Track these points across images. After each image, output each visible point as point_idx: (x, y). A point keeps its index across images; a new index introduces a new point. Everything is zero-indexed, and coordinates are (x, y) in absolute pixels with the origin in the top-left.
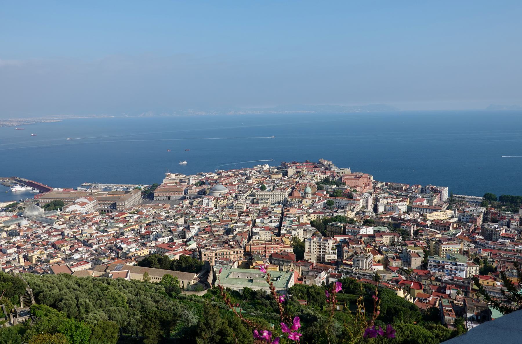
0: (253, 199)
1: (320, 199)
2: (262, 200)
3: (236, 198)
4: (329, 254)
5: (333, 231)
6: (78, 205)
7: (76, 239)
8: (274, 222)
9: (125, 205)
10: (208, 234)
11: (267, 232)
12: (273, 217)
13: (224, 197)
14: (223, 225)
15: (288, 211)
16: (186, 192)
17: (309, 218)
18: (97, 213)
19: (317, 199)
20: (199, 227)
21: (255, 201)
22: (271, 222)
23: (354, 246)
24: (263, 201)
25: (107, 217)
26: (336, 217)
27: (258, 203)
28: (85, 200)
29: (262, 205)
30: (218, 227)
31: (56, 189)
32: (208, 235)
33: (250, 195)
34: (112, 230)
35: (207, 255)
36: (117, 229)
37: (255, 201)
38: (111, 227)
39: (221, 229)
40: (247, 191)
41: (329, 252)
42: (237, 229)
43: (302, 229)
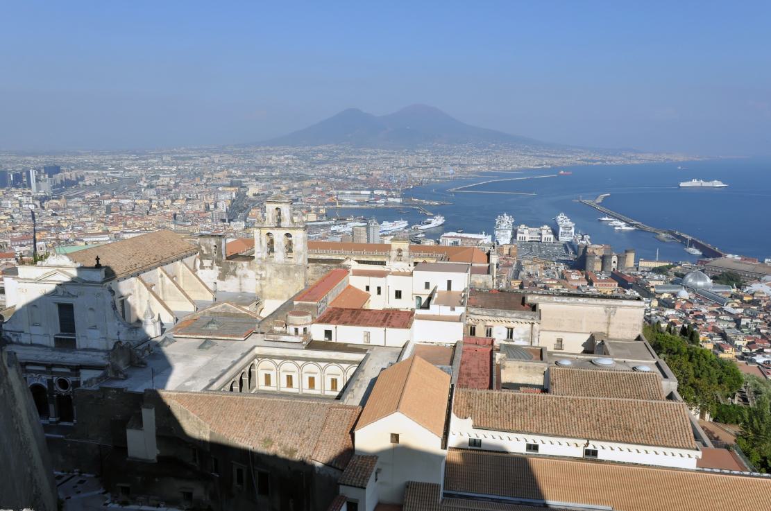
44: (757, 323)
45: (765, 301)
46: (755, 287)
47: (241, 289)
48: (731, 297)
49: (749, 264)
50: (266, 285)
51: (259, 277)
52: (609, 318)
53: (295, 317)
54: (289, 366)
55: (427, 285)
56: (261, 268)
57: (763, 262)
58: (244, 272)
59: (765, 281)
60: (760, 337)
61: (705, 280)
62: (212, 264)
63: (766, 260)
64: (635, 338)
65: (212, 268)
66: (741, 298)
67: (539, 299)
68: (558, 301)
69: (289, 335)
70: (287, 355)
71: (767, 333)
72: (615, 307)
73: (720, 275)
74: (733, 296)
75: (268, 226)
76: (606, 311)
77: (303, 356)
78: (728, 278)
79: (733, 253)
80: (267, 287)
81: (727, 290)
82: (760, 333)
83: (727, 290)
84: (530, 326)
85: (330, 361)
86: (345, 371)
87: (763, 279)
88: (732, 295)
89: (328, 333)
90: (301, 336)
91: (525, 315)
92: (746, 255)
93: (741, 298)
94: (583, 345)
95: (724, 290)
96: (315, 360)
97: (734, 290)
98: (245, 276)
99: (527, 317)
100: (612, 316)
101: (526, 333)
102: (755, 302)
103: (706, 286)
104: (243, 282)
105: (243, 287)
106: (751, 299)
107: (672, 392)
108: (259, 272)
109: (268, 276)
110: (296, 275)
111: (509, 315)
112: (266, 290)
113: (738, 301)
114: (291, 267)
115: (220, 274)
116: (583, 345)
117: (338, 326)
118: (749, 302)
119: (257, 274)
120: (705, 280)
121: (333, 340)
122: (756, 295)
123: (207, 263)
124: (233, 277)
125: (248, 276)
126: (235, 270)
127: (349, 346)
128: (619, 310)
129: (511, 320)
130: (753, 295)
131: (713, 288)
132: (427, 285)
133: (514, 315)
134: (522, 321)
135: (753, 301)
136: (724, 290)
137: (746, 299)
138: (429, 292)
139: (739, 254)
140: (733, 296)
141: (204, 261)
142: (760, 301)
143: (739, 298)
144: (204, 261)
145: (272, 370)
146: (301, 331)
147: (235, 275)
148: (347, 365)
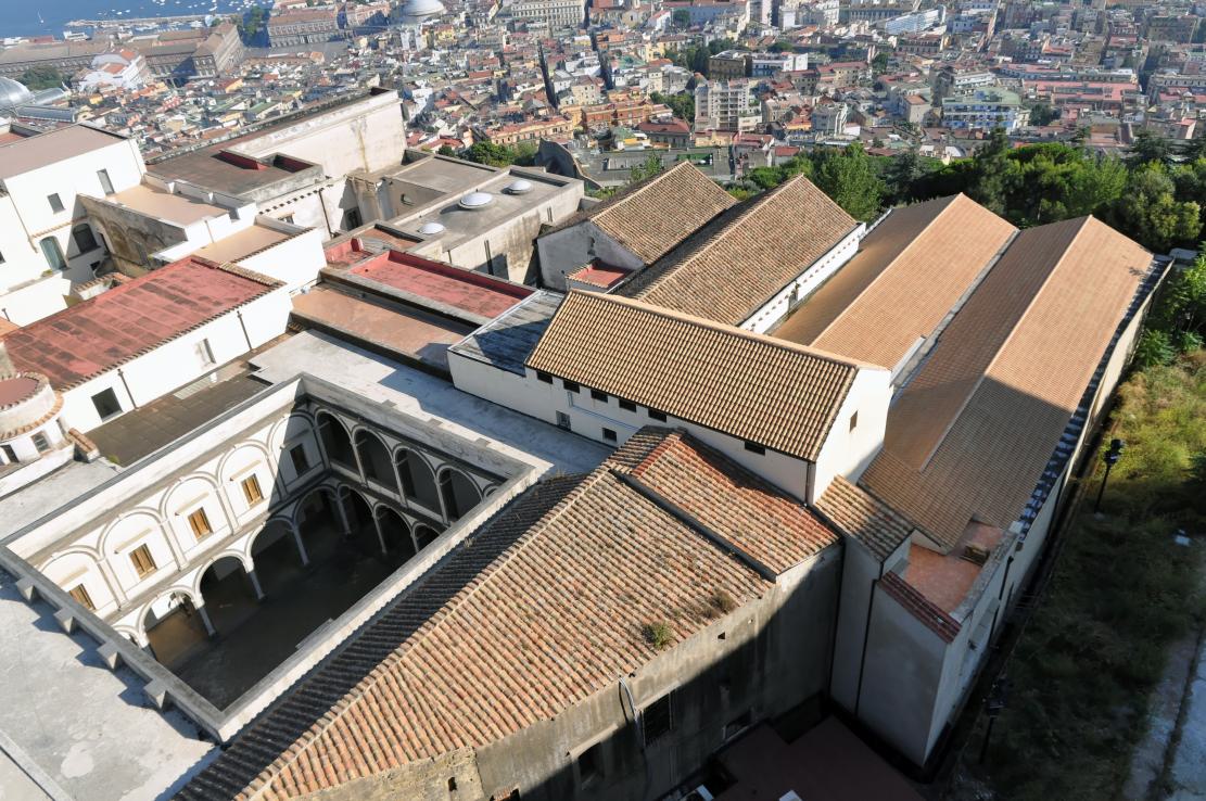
0: (512, 23)
1: (657, 10)
2: (533, 22)
3: (469, 22)
4: (744, 115)
5: (723, 69)
6: (105, 71)
7: (156, 144)
8: (589, 66)
9: (214, 63)
10: (458, 103)
11: (589, 87)
12: (583, 54)
13: (445, 22)
14: (479, 82)
15: (606, 39)
16: (342, 21)
17: (655, 50)
18: (162, 86)
19: (653, 10)
20: (430, 91)
21: (517, 25)
22: (582, 65)
23: (787, 95)
24: (537, 25)
25: (191, 92)
26: (711, 44)
27: (524, 30)
28: (116, 58)
29: (536, 34)
30: (470, 89)
31: (8, 41)
32: (459, 106)
33: (498, 15)
34: (228, 117)
35: (559, 130)
36: (238, 115)
37: (517, 25)
38: (221, 113)
39: (479, 92)
40: (491, 6)
41: (745, 112)
42: (518, 88)
43: (660, 75)
44: (140, 131)
45: (122, 97)
46: (92, 79)
48: (71, 105)
49: (46, 47)
52: (361, 138)
53: (15, 409)
54: (129, 530)
55: (56, 202)
57: (63, 38)
59: (99, 66)
60: (159, 149)
61: (18, 89)
63: (67, 34)
64: (401, 158)
66: (85, 101)
67: (247, 149)
68: (279, 139)
69: (25, 464)
70: (112, 504)
71: (164, 140)
72: (363, 116)
73: (25, 76)
74: (75, 103)
76: (353, 129)
77: (158, 478)
78: (40, 77)
79: (13, 36)
81: (59, 96)
82: (156, 144)
83: (59, 96)
84: (317, 196)
85: (227, 445)
86: (265, 447)
87: (94, 62)
88: (70, 101)
89: (106, 403)
90: (62, 447)
91: (301, 179)
92: (36, 35)
93: (85, 101)
94: (340, 206)
95: (55, 98)
96: (189, 468)
97: (68, 93)
99: (307, 181)
100: (363, 134)
101: (315, 214)
102: (110, 102)
103: (25, 100)
106: (100, 99)
107: (581, 200)
111: (274, 192)
113: (85, 108)
116: (340, 206)
117: (125, 368)
118: (101, 105)
120: (18, 89)
121: (126, 406)
122: (102, 91)
127: (181, 395)
128: (370, 118)
129: (284, 200)
130: (98, 92)
131: (38, 98)
132: (56, 202)
133: (284, 189)
134: (304, 192)
135: (105, 101)
136: (55, 98)
137: (95, 101)
138: (67, 215)
139: (24, 35)
140: (75, 103)
142: (114, 98)
143: (84, 104)
145: (84, 570)
146: (53, 433)
148: (266, 430)
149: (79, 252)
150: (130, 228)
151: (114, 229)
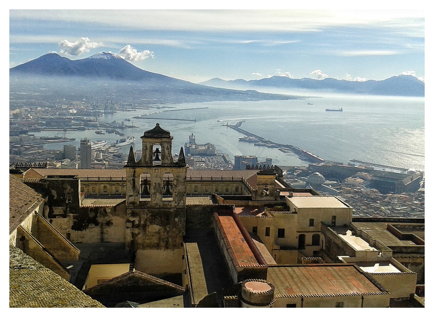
47: (102, 239)
50: (139, 233)
51: (129, 225)
56: (134, 214)
58: (107, 218)
62: (65, 212)
65: (64, 216)
75: (144, 165)
80: (139, 236)
98: (109, 223)
104: (105, 230)
105: (106, 236)
108: (132, 219)
109: (142, 222)
110: (177, 219)
112: (140, 239)
114: (172, 210)
115: (75, 223)
119: (128, 221)
123: (58, 210)
124: (92, 225)
125: (112, 223)
126: (96, 216)
141: (54, 208)
144: (54, 208)
147: (97, 224)
149: (311, 243)
150: (334, 242)
151: (328, 240)
